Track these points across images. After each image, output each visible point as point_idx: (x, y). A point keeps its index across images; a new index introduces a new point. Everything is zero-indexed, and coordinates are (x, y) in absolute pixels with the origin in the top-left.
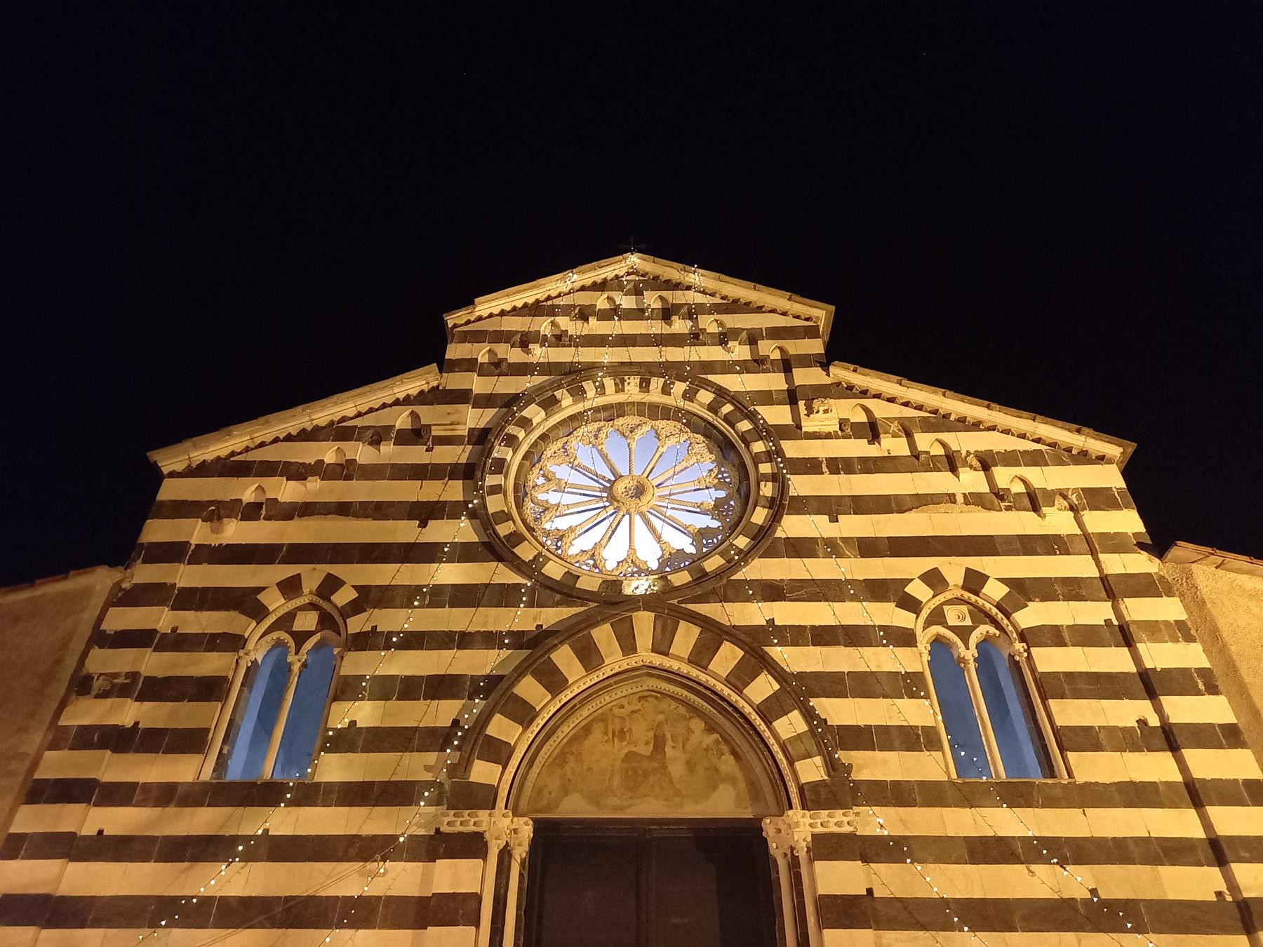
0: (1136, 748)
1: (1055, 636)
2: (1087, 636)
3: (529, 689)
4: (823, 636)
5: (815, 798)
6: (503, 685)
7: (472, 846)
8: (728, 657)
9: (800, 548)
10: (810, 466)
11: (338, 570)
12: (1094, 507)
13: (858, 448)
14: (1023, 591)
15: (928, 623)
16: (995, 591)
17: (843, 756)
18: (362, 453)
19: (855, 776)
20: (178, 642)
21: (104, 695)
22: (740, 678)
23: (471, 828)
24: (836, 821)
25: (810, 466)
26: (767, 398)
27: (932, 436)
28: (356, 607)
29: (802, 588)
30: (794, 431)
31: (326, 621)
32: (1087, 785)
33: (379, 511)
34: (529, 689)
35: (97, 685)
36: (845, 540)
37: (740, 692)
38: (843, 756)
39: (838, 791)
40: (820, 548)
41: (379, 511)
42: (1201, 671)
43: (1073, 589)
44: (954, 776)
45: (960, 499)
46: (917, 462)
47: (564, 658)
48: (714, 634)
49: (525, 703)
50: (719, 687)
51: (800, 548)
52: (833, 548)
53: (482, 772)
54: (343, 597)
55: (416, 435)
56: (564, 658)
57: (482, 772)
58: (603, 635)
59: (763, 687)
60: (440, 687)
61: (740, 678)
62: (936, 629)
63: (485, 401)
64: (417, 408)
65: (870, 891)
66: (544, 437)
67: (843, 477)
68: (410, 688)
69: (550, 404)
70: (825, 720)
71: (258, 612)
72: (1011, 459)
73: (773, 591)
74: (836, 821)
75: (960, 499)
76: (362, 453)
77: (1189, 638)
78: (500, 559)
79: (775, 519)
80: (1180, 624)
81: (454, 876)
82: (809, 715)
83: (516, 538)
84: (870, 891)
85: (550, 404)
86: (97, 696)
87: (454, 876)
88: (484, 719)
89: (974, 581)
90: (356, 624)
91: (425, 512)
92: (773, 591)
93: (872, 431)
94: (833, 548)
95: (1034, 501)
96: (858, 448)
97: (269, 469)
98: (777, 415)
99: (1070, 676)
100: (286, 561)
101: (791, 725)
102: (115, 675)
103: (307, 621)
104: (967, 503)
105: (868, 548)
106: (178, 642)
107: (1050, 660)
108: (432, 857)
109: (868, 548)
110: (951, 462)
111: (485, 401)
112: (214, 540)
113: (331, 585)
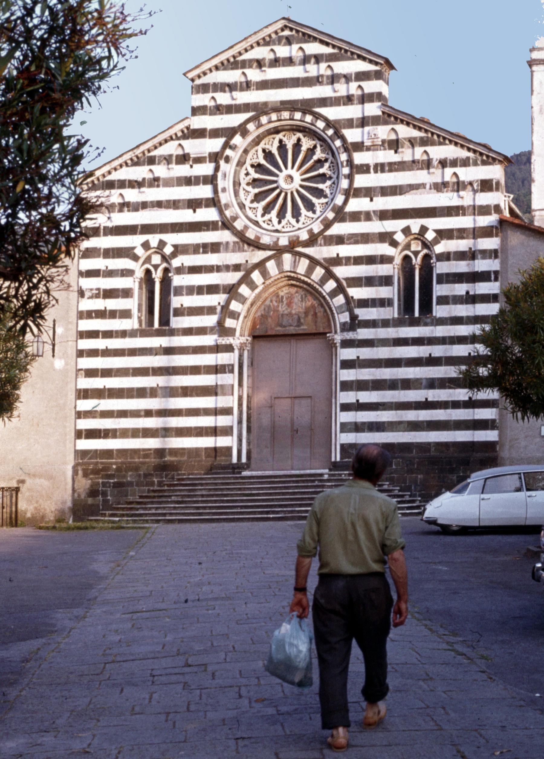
0: (461, 303)
1: (446, 257)
2: (461, 256)
3: (244, 290)
4: (358, 260)
5: (345, 327)
6: (234, 290)
7: (229, 348)
8: (319, 272)
9: (355, 217)
10: (364, 169)
11: (165, 237)
12: (482, 191)
13: (387, 156)
14: (442, 234)
15: (402, 250)
16: (430, 236)
17: (357, 311)
18: (160, 171)
19: (360, 318)
20: (110, 273)
21: (91, 297)
22: (323, 281)
23: (228, 343)
24: (350, 335)
25: (364, 169)
26: (350, 123)
27: (423, 149)
28: (174, 255)
29: (352, 238)
30: (359, 147)
31: (164, 258)
32: (440, 318)
33: (175, 204)
34: (244, 290)
35: (88, 294)
36: (374, 212)
37: (322, 287)
38: (357, 311)
39: (355, 323)
40: (362, 217)
41: (175, 204)
42: (496, 273)
43: (461, 233)
44: (396, 316)
45: (428, 186)
46: (413, 165)
47: (256, 276)
48: (314, 262)
49: (242, 296)
50: (315, 285)
51: (355, 217)
52: (368, 216)
53: (229, 323)
54: (168, 250)
55: (183, 159)
56: (256, 276)
57: (229, 323)
58: (271, 265)
59: (331, 285)
60: (212, 289)
61: (323, 281)
62: (407, 252)
63: (215, 133)
64: (183, 142)
65: (358, 357)
66: (246, 152)
67: (379, 174)
68: (200, 290)
69: (244, 132)
70: (352, 297)
71: (136, 258)
72: (454, 163)
73: (340, 240)
74: (350, 335)
75: (428, 186)
76: (160, 171)
77: (496, 257)
78: (228, 229)
79: (346, 202)
80: (496, 251)
81: (223, 358)
82: (346, 296)
83: (235, 218)
84: (358, 357)
85: (244, 132)
86: (88, 298)
87: (223, 358)
88: (228, 302)
89: (424, 229)
90: (176, 263)
91: (194, 204)
92: (340, 240)
93: (394, 145)
94: (368, 216)
95: (459, 186)
96: (387, 156)
97: (122, 184)
98: (353, 135)
99: (448, 275)
100: (142, 233)
101: (340, 300)
102: (91, 290)
103: (156, 259)
104: (430, 189)
105: (384, 215)
106: (110, 273)
107: (441, 268)
108: (217, 352)
109: (384, 215)
110: (428, 164)
111: (215, 133)
112: (110, 224)
113: (162, 244)
